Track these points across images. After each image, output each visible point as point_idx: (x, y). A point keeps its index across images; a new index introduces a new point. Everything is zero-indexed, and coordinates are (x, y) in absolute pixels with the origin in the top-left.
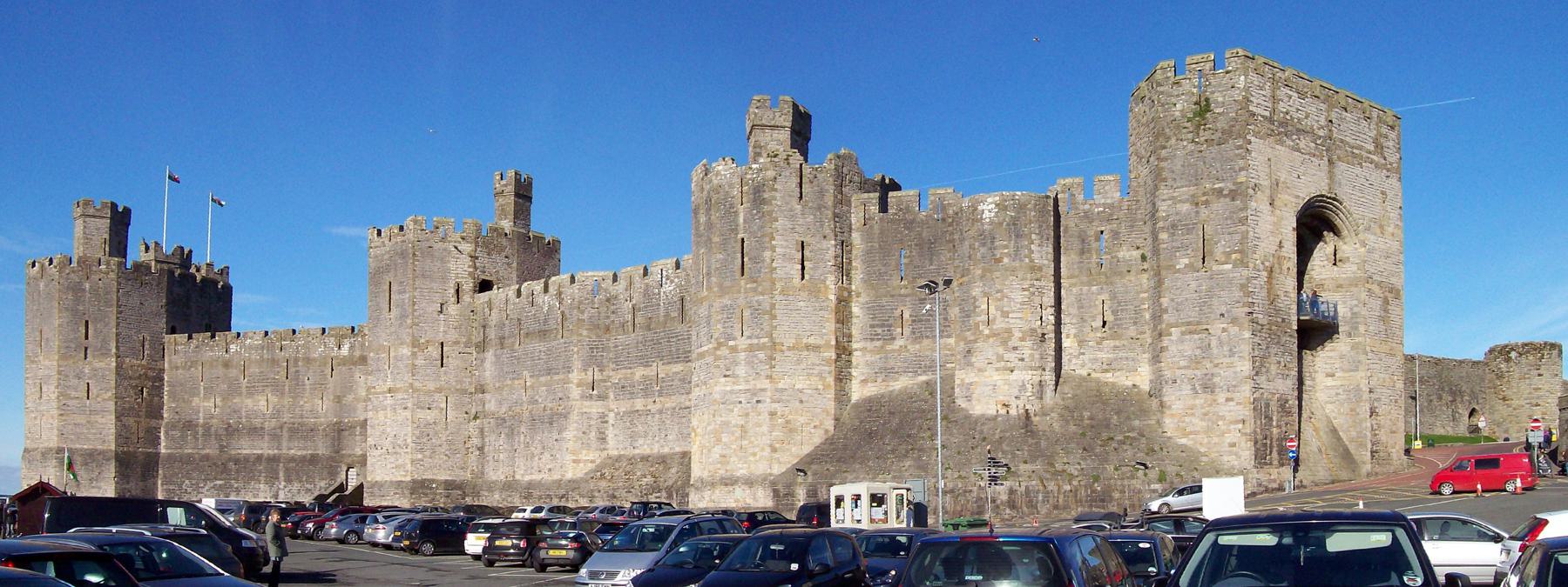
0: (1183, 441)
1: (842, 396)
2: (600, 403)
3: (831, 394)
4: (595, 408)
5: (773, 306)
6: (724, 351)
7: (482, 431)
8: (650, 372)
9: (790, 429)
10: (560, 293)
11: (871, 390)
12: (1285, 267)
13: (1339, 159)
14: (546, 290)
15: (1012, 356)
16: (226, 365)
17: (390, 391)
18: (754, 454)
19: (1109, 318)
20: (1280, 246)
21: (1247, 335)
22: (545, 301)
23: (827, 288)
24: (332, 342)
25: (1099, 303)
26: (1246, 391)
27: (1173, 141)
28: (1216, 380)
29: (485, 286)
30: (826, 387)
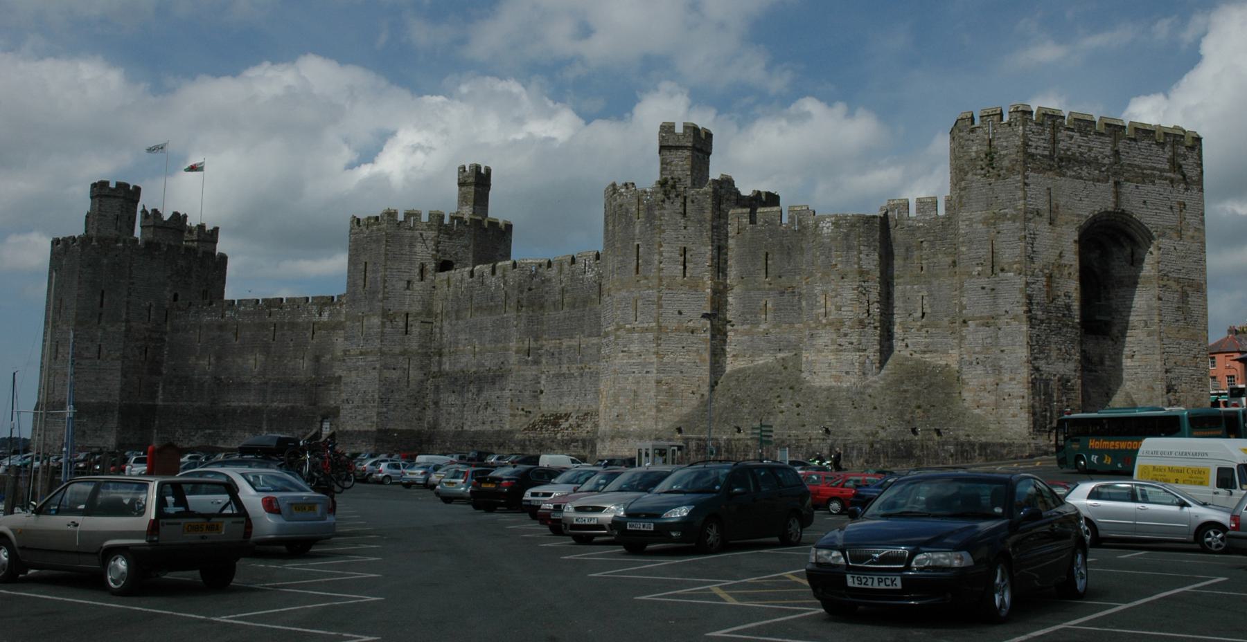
0: (977, 411)
1: (716, 368)
2: (534, 367)
3: (707, 367)
4: (530, 372)
5: (660, 298)
6: (621, 333)
7: (437, 387)
8: (574, 343)
9: (671, 393)
10: (504, 276)
11: (741, 364)
12: (1066, 272)
13: (1127, 180)
14: (493, 272)
15: (843, 341)
16: (221, 327)
17: (361, 354)
18: (644, 414)
19: (928, 310)
20: (1061, 256)
21: (1025, 328)
22: (492, 281)
23: (704, 283)
24: (314, 309)
25: (919, 298)
26: (1024, 374)
27: (969, 176)
28: (1002, 363)
29: (445, 266)
30: (703, 361)
